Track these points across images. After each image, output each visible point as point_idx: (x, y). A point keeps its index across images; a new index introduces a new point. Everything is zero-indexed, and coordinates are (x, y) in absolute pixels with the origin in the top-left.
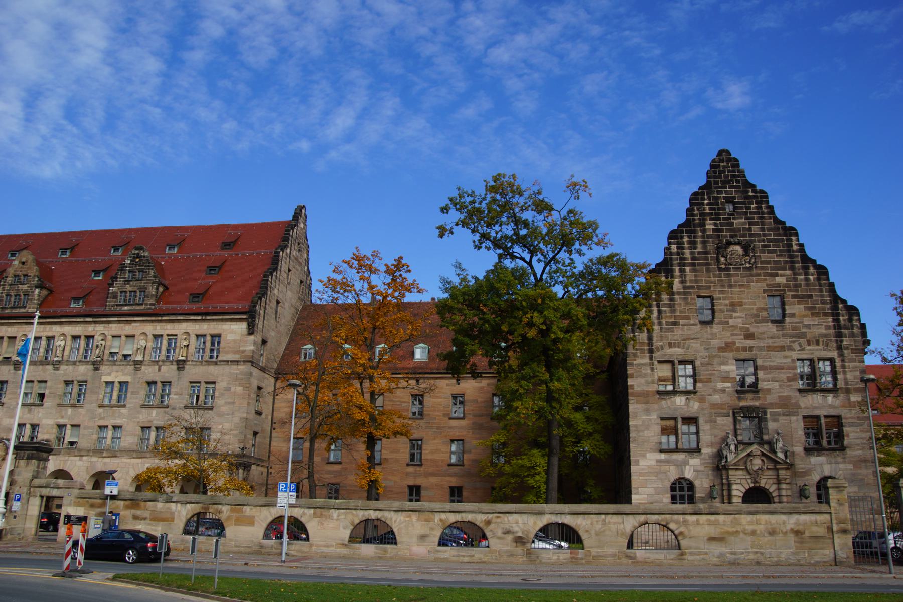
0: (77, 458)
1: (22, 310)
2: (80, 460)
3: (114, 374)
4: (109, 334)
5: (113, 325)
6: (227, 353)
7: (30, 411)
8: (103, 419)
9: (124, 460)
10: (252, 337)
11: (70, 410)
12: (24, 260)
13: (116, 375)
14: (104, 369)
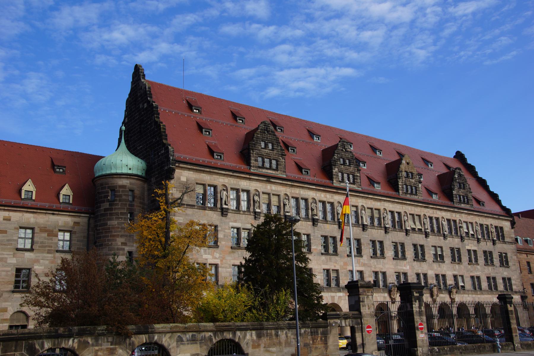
0: (467, 295)
1: (416, 197)
2: (469, 296)
3: (470, 245)
4: (462, 220)
5: (463, 215)
6: (507, 237)
7: (439, 265)
8: (471, 272)
9: (485, 296)
10: (513, 230)
11: (457, 266)
12: (408, 161)
13: (470, 245)
14: (466, 240)
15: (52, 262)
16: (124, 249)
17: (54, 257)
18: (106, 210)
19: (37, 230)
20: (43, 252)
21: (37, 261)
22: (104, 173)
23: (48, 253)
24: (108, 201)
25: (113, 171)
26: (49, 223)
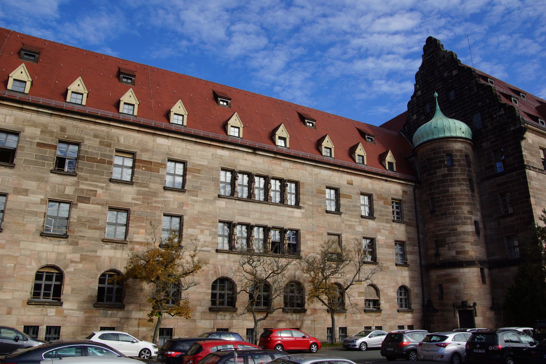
15: (391, 233)
16: (471, 218)
17: (392, 228)
18: (444, 176)
19: (375, 197)
20: (382, 222)
21: (378, 230)
22: (436, 137)
23: (387, 222)
24: (446, 166)
25: (447, 134)
26: (384, 191)
